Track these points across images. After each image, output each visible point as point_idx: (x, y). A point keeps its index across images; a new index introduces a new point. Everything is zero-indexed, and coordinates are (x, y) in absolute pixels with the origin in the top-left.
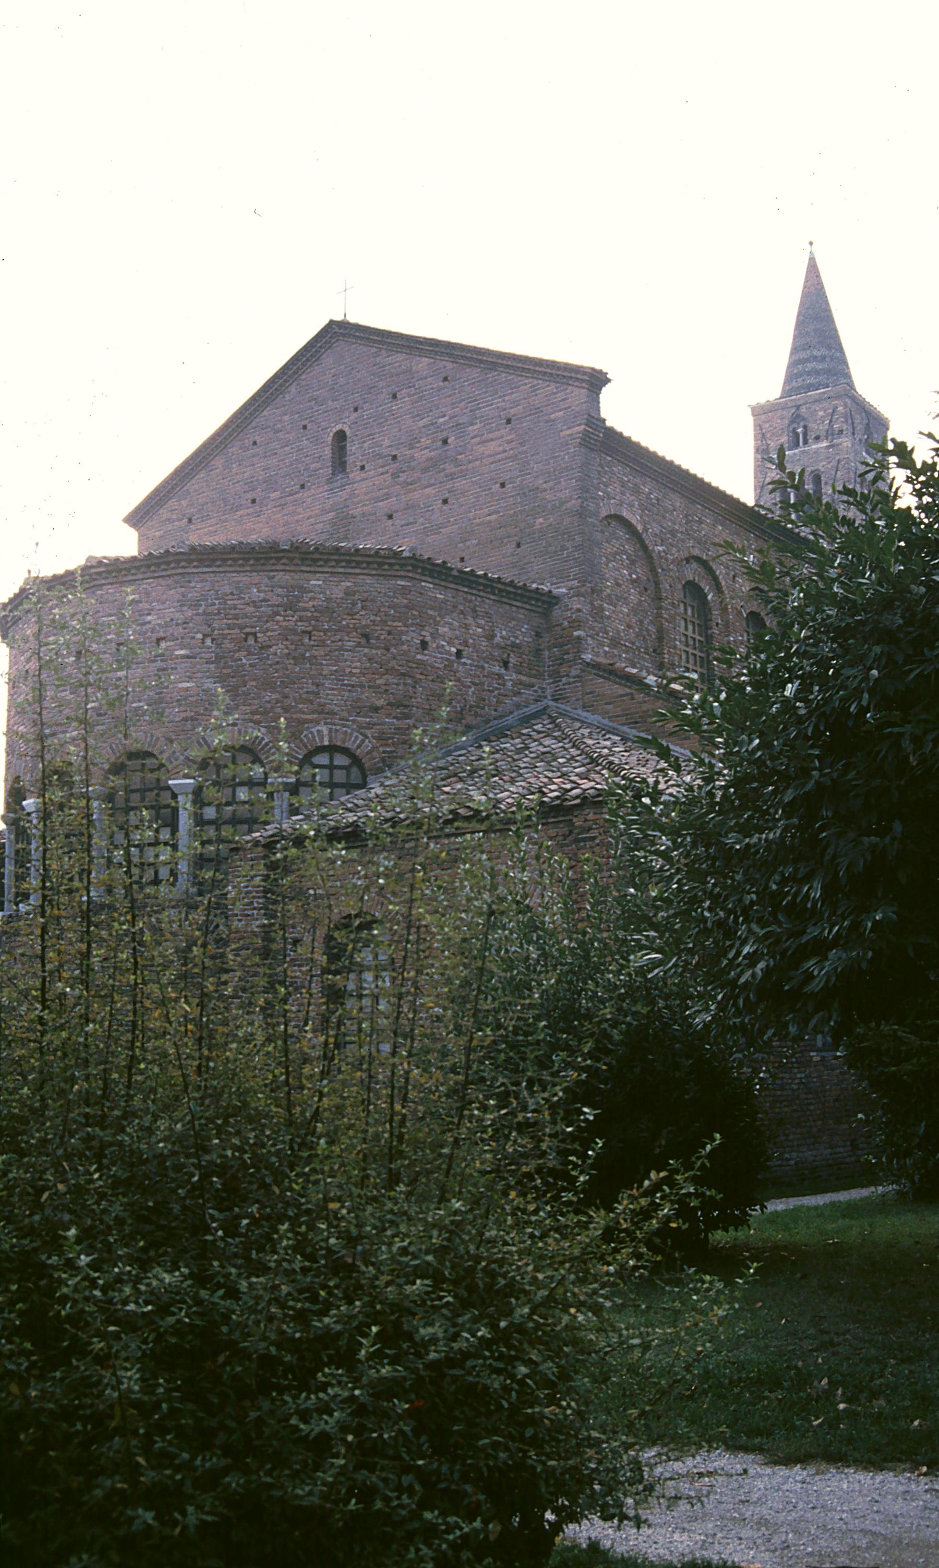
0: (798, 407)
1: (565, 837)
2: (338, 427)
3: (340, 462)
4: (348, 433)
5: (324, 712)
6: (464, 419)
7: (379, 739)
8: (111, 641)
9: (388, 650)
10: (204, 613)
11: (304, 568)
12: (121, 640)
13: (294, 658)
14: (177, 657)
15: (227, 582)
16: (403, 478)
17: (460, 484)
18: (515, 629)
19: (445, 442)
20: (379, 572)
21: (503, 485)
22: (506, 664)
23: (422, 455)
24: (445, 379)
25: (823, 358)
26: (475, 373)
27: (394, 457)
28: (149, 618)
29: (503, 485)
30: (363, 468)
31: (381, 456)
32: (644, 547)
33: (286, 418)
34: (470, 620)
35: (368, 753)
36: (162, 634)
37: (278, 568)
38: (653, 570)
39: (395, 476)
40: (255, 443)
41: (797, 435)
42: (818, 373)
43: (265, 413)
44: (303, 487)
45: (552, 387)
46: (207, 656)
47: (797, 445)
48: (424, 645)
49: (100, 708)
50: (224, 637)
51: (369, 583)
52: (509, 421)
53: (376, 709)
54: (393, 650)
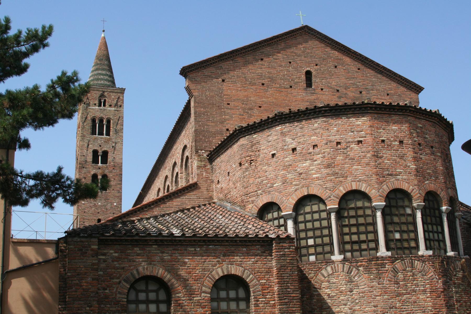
0: (104, 92)
2: (308, 69)
3: (309, 83)
6: (370, 87)
8: (415, 141)
14: (438, 156)
19: (361, 92)
24: (359, 69)
27: (338, 91)
30: (322, 89)
31: (331, 88)
43: (267, 49)
47: (100, 105)
52: (388, 95)
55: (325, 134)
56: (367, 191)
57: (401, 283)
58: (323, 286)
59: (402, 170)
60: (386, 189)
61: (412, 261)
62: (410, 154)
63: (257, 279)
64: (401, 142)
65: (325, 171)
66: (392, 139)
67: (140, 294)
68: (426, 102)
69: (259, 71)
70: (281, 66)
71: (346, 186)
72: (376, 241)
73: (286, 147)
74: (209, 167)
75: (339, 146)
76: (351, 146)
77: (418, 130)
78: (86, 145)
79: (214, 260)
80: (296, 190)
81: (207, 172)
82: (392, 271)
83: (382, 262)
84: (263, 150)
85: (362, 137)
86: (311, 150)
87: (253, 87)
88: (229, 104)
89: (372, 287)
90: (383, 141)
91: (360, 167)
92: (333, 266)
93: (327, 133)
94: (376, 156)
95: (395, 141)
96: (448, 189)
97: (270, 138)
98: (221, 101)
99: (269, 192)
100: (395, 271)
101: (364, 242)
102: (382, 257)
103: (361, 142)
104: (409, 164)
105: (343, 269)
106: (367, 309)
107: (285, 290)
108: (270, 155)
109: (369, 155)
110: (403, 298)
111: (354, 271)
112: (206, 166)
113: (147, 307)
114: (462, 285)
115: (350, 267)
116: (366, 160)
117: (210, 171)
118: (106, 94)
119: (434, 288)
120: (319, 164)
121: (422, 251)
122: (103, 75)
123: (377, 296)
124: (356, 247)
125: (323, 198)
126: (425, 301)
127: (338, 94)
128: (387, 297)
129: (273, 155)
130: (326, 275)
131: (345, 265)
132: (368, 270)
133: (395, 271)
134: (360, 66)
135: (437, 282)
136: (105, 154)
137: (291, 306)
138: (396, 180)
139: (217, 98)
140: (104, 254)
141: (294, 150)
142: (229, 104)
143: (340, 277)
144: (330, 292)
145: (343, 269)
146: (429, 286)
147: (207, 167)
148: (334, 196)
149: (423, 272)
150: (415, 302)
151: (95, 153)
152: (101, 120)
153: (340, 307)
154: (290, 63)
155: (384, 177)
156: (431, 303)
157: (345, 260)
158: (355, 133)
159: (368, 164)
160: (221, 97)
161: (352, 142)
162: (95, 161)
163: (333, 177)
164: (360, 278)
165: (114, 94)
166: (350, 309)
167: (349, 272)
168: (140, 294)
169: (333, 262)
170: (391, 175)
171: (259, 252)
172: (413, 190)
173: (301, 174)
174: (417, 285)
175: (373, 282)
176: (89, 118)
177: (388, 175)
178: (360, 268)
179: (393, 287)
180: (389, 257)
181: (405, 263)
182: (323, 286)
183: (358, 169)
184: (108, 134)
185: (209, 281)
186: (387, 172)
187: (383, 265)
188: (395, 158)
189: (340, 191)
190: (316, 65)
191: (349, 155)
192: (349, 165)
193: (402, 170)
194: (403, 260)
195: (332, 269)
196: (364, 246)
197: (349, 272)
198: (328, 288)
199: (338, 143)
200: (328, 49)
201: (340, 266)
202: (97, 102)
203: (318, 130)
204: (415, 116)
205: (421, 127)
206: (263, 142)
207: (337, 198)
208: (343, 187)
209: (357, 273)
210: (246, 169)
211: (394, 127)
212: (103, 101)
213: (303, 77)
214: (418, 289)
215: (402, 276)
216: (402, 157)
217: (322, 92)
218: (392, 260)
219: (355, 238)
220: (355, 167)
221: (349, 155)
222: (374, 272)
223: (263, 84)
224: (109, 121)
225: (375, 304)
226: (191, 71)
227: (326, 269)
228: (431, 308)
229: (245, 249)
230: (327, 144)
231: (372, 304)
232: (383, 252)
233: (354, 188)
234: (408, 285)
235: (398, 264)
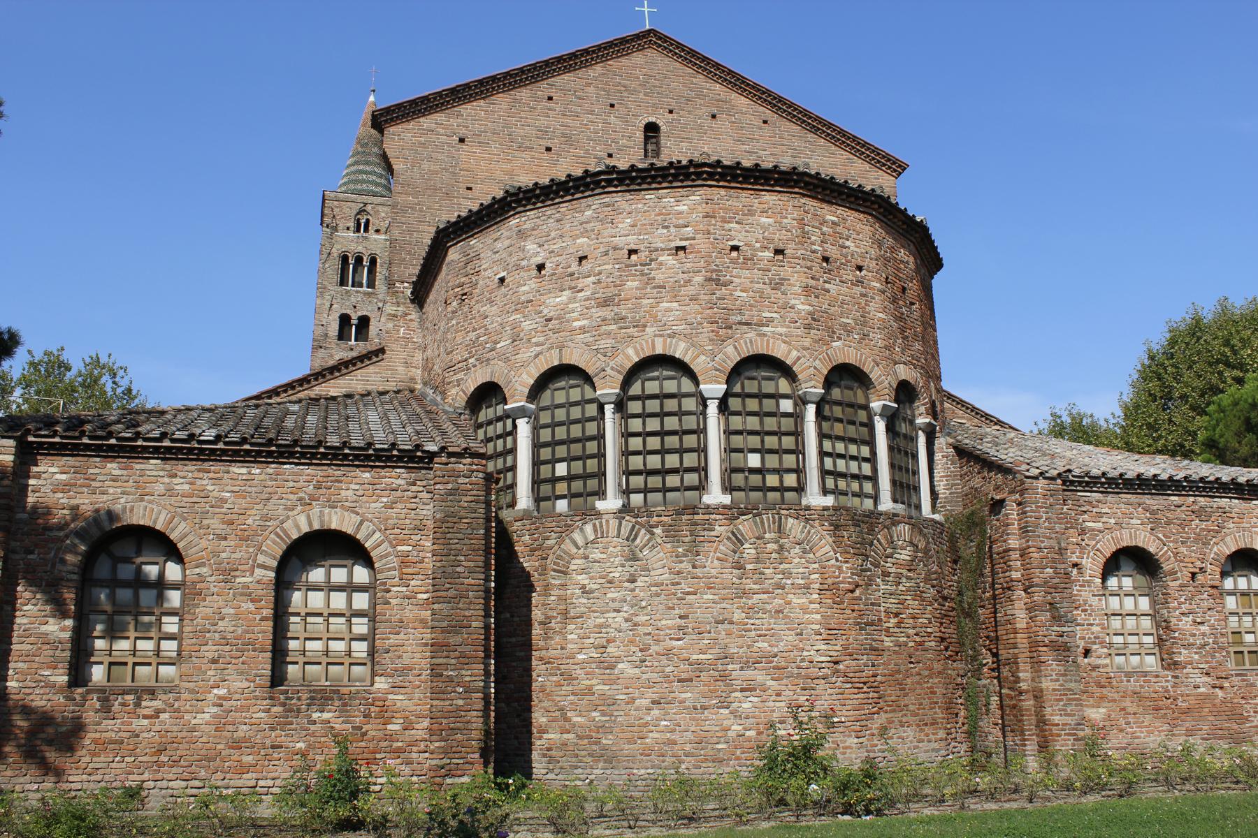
0: (366, 204)
4: (663, 128)
8: (814, 252)
14: (873, 288)
24: (765, 122)
33: (591, 90)
41: (359, 225)
45: (867, 166)
47: (358, 230)
55: (605, 232)
56: (687, 359)
57: (749, 567)
58: (572, 567)
59: (775, 315)
60: (732, 355)
61: (780, 519)
62: (797, 278)
63: (390, 543)
65: (597, 313)
66: (758, 245)
67: (120, 566)
68: (909, 195)
69: (543, 122)
70: (591, 112)
71: (641, 345)
72: (702, 470)
73: (524, 263)
74: (414, 315)
75: (634, 257)
76: (661, 258)
77: (824, 229)
78: (328, 305)
79: (292, 496)
80: (536, 356)
81: (408, 328)
82: (728, 538)
83: (707, 517)
84: (485, 270)
85: (687, 239)
86: (574, 267)
87: (527, 155)
88: (470, 189)
89: (679, 573)
90: (735, 248)
91: (675, 304)
92: (597, 522)
93: (610, 230)
94: (716, 281)
96: (896, 363)
97: (499, 245)
98: (453, 182)
99: (488, 360)
100: (738, 540)
101: (674, 471)
102: (708, 507)
103: (678, 249)
104: (793, 302)
105: (619, 531)
106: (664, 622)
107: (450, 570)
108: (497, 281)
109: (699, 279)
110: (750, 602)
111: (643, 536)
112: (406, 315)
113: (136, 596)
114: (909, 578)
115: (633, 527)
116: (691, 290)
117: (415, 324)
118: (369, 208)
119: (830, 581)
120: (588, 299)
121: (815, 498)
122: (366, 173)
123: (689, 593)
124: (655, 481)
125: (590, 371)
126: (805, 610)
128: (711, 597)
129: (502, 280)
130: (580, 542)
131: (624, 522)
132: (672, 533)
133: (738, 540)
134: (767, 113)
135: (840, 568)
136: (364, 322)
137: (461, 605)
138: (759, 335)
139: (446, 177)
141: (541, 267)
142: (470, 189)
143: (611, 549)
144: (586, 582)
145: (619, 531)
146: (817, 576)
147: (409, 317)
148: (612, 368)
149: (808, 547)
150: (778, 612)
151: (345, 320)
152: (359, 260)
153: (607, 615)
154: (612, 106)
155: (731, 328)
156: (818, 617)
157: (626, 509)
158: (672, 230)
159: (694, 299)
160: (454, 174)
161: (662, 250)
162: (343, 335)
163: (614, 327)
164: (654, 552)
165: (386, 209)
166: (627, 620)
167: (632, 537)
168: (120, 566)
169: (598, 514)
170: (747, 324)
171: (403, 482)
172: (799, 358)
173: (549, 320)
174: (787, 574)
175: (681, 562)
176: (335, 253)
177: (740, 323)
178: (655, 530)
179: (731, 576)
180: (725, 507)
181: (762, 522)
182: (572, 567)
183: (671, 310)
184: (371, 284)
185: (274, 542)
186: (739, 318)
187: (709, 526)
188: (761, 286)
189: (628, 357)
190: (671, 112)
191: (654, 278)
192: (651, 301)
193: (775, 315)
194: (759, 515)
195: (595, 531)
196: (673, 480)
197: (632, 537)
198: (583, 571)
199: (632, 252)
200: (700, 79)
201: (614, 523)
202: (351, 224)
203: (592, 224)
205: (833, 223)
206: (486, 254)
207: (619, 372)
208: (635, 348)
209: (649, 540)
210: (453, 312)
211: (764, 220)
212: (363, 221)
213: (640, 135)
214: (789, 582)
215: (753, 551)
216: (777, 285)
218: (732, 513)
219: (654, 461)
220: (665, 304)
221: (654, 278)
222: (687, 539)
223: (549, 149)
224: (373, 261)
225: (682, 612)
226: (392, 119)
227: (582, 530)
228: (817, 627)
229: (367, 475)
230: (606, 253)
231: (677, 611)
232: (715, 496)
233: (659, 351)
234: (767, 571)
235: (745, 525)
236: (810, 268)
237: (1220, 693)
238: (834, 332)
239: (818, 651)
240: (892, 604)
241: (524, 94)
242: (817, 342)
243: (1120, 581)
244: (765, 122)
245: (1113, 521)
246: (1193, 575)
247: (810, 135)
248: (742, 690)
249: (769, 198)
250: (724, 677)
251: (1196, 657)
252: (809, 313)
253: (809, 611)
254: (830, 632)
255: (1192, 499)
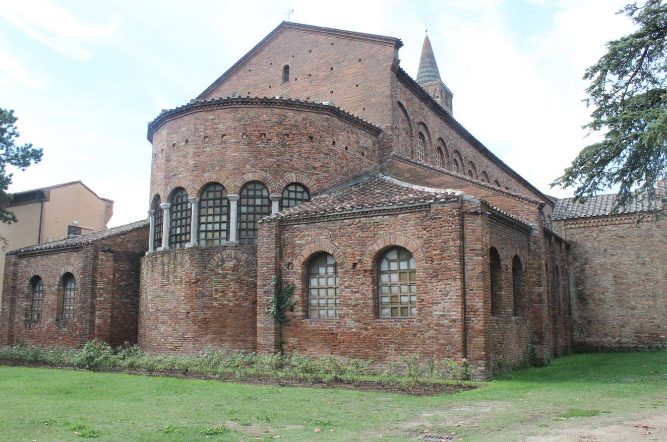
1: (424, 217)
2: (286, 64)
3: (286, 78)
4: (290, 66)
5: (294, 169)
6: (340, 60)
7: (316, 180)
8: (201, 136)
9: (320, 143)
10: (244, 125)
11: (285, 107)
12: (206, 135)
13: (282, 145)
15: (253, 111)
16: (314, 83)
17: (338, 85)
18: (367, 141)
19: (332, 69)
20: (317, 111)
21: (357, 86)
22: (363, 154)
23: (321, 74)
24: (332, 44)
25: (431, 71)
26: (345, 41)
27: (310, 75)
28: (219, 126)
29: (357, 86)
30: (296, 79)
31: (304, 75)
32: (407, 116)
33: (264, 60)
34: (350, 135)
35: (312, 186)
36: (224, 133)
37: (275, 106)
38: (410, 125)
39: (310, 82)
40: (250, 70)
42: (429, 76)
44: (270, 87)
45: (379, 47)
46: (244, 142)
48: (334, 143)
49: (196, 164)
50: (252, 134)
51: (313, 116)
52: (360, 60)
53: (315, 168)
54: (322, 144)
64: (187, 141)
95: (183, 141)
127: (310, 78)
134: (333, 39)
135: (192, 273)
140: (22, 264)
154: (271, 64)
204: (206, 109)
205: (212, 119)
213: (281, 73)
216: (185, 156)
217: (296, 82)
236: (197, 144)
237: (365, 332)
238: (206, 170)
239: (183, 308)
240: (220, 287)
241: (241, 73)
242: (196, 176)
243: (327, 270)
244: (332, 44)
245: (310, 238)
246: (355, 265)
247: (353, 42)
248: (161, 323)
249: (186, 118)
250: (157, 318)
251: (351, 311)
252: (194, 164)
253: (181, 291)
254: (189, 299)
255: (357, 220)
